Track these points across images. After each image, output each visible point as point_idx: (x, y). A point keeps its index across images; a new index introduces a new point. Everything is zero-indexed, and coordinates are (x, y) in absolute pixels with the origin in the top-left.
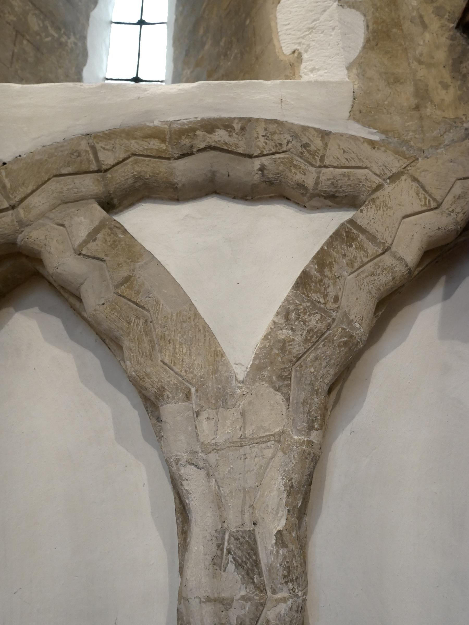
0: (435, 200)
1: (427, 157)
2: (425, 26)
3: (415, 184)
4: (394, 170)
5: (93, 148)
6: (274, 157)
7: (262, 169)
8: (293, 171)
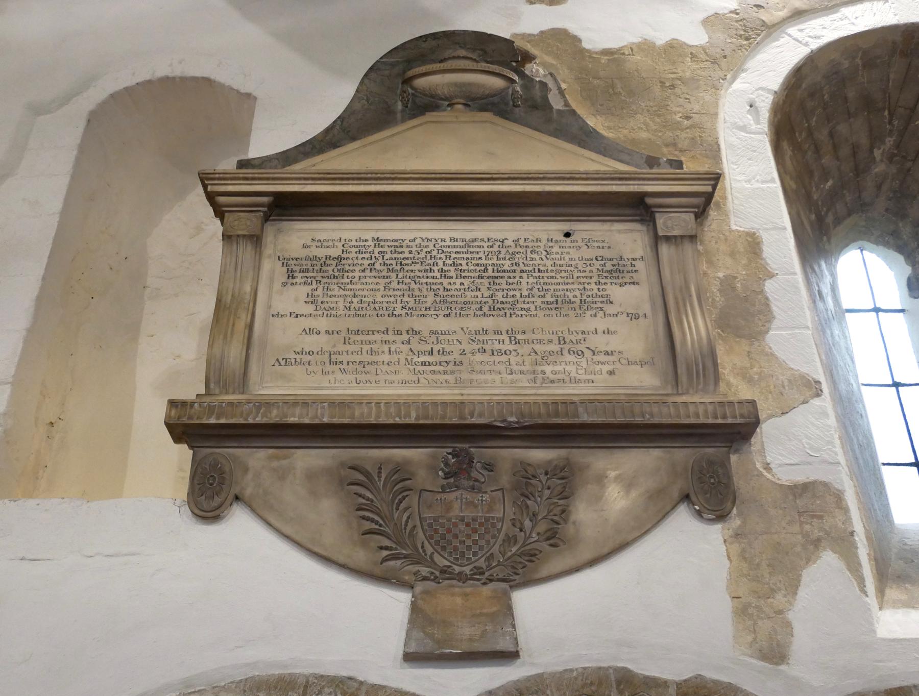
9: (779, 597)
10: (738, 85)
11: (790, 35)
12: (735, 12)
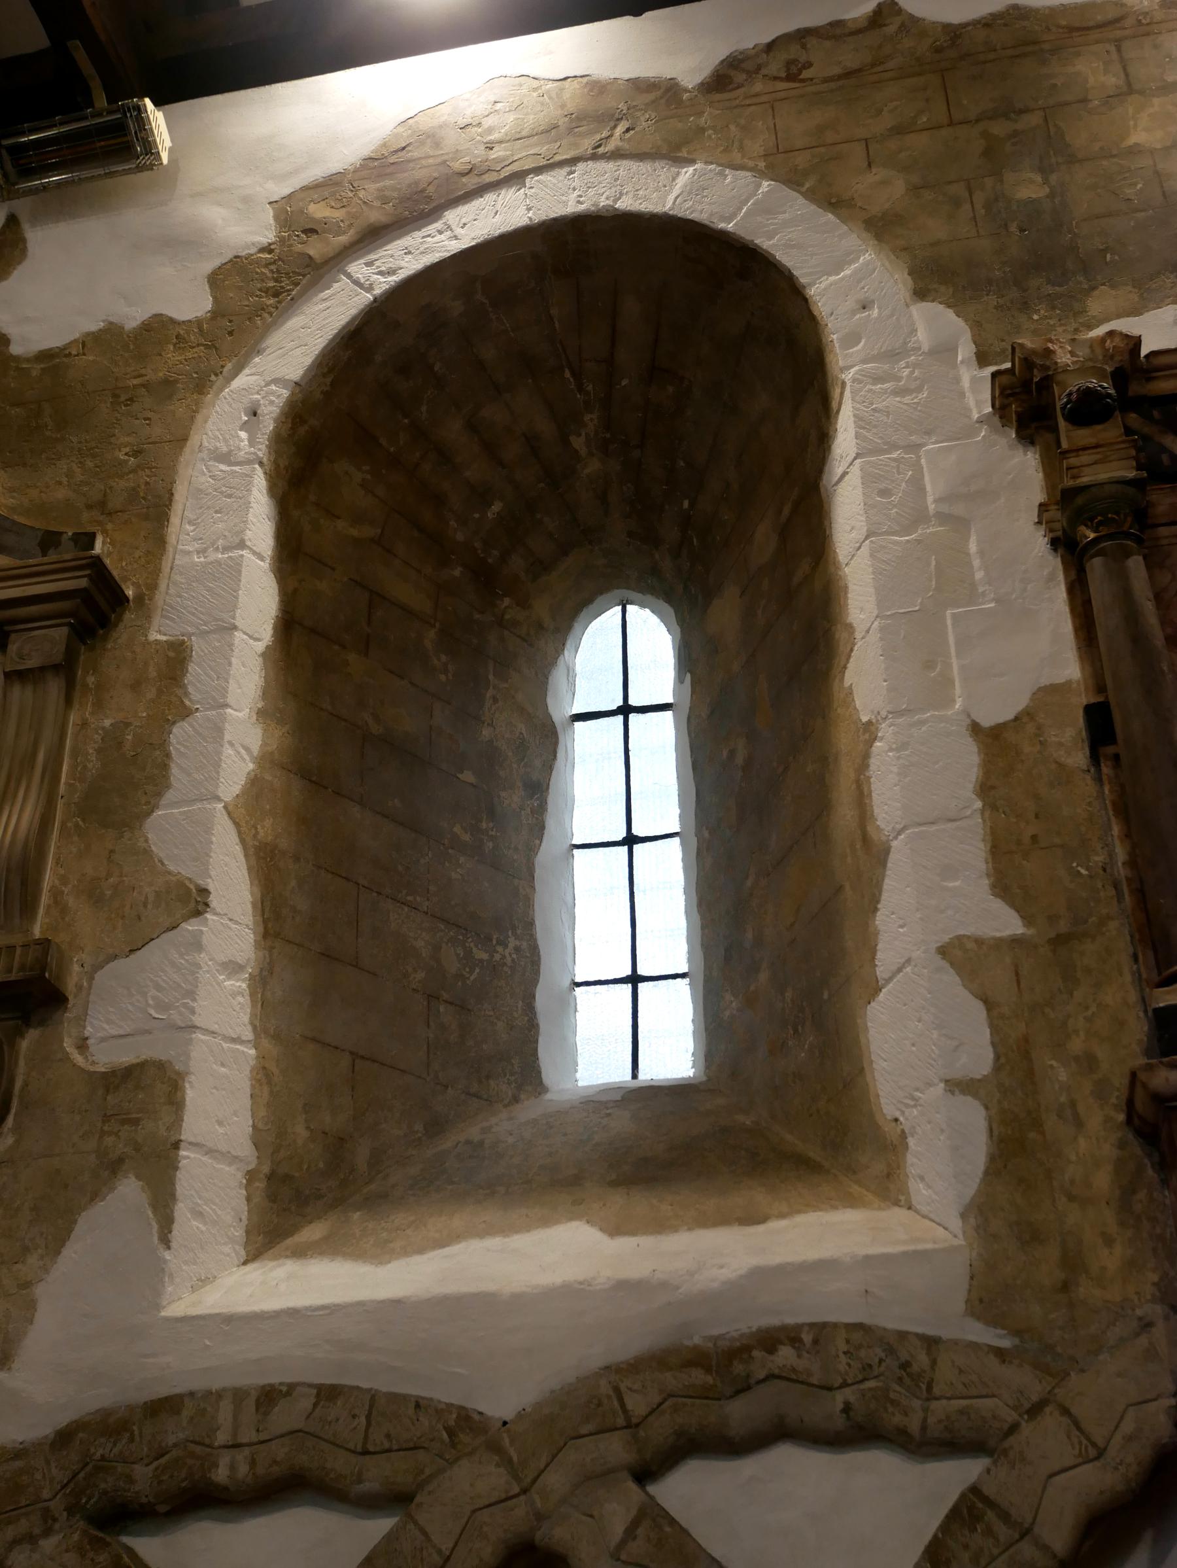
0: (1094, 1445)
1: (1083, 1371)
2: (1079, 1123)
3: (1065, 1420)
4: (1035, 1398)
5: (617, 1390)
6: (862, 1386)
7: (847, 1409)
8: (890, 1409)
9: (33, 1260)
10: (243, 380)
11: (349, 276)
12: (267, 249)
